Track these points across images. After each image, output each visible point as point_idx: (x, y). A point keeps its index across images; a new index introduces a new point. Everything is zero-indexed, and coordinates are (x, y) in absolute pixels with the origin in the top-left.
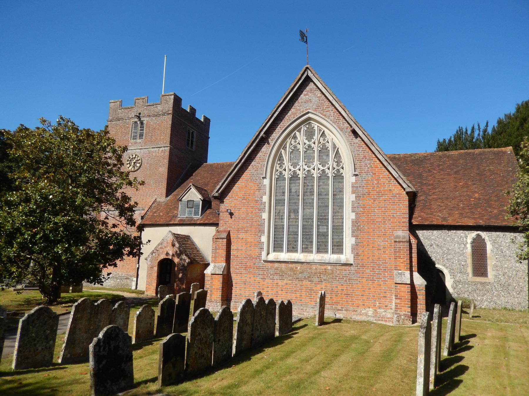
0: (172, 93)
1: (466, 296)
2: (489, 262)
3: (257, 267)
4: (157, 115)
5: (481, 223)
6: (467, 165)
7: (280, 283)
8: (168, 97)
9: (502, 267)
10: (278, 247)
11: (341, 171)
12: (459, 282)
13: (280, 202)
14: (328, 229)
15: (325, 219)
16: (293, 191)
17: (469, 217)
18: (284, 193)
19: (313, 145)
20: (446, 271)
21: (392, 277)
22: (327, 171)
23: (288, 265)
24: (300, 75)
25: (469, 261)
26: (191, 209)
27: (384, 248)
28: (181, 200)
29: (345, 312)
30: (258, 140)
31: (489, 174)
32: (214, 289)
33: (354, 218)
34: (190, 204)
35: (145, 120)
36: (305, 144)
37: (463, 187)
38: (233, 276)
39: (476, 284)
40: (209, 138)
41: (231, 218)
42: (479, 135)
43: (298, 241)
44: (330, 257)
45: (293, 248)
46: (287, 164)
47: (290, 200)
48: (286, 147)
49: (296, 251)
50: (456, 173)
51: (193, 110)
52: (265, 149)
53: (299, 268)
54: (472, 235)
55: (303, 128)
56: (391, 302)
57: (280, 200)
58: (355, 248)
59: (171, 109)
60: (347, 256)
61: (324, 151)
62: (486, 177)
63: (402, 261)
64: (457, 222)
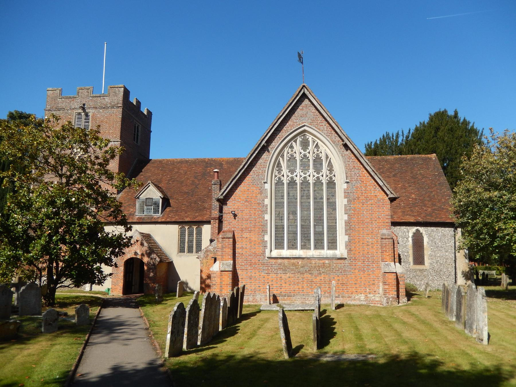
0: (122, 86)
1: (408, 282)
2: (425, 252)
3: (261, 263)
4: (105, 108)
5: (420, 219)
6: (402, 169)
7: (283, 276)
8: (117, 89)
9: (435, 256)
10: (279, 245)
11: (334, 178)
13: (279, 205)
14: (323, 228)
15: (321, 220)
16: (291, 195)
17: (410, 215)
18: (283, 196)
19: (308, 155)
21: (379, 268)
22: (321, 178)
23: (290, 260)
24: (298, 92)
25: (411, 252)
26: (149, 207)
27: (372, 244)
28: (138, 198)
29: (342, 299)
30: (260, 148)
31: (420, 177)
32: (224, 285)
33: (347, 219)
34: (149, 201)
35: (91, 112)
36: (301, 153)
37: (401, 188)
38: (239, 272)
39: (415, 271)
40: (151, 132)
41: (235, 219)
42: (403, 140)
43: (297, 239)
44: (326, 252)
45: (293, 245)
47: (288, 203)
48: (284, 155)
49: (296, 248)
50: (394, 176)
52: (265, 156)
53: (300, 263)
54: (414, 229)
55: (299, 139)
56: (378, 288)
57: (279, 203)
58: (349, 245)
59: (121, 102)
60: (341, 251)
61: (318, 161)
62: (418, 180)
63: (387, 254)
64: (402, 219)
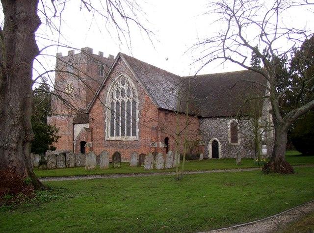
12: (225, 146)
20: (218, 141)
25: (229, 135)
44: (131, 138)
46: (115, 97)
51: (101, 53)
54: (231, 121)
60: (137, 137)
61: (128, 90)
